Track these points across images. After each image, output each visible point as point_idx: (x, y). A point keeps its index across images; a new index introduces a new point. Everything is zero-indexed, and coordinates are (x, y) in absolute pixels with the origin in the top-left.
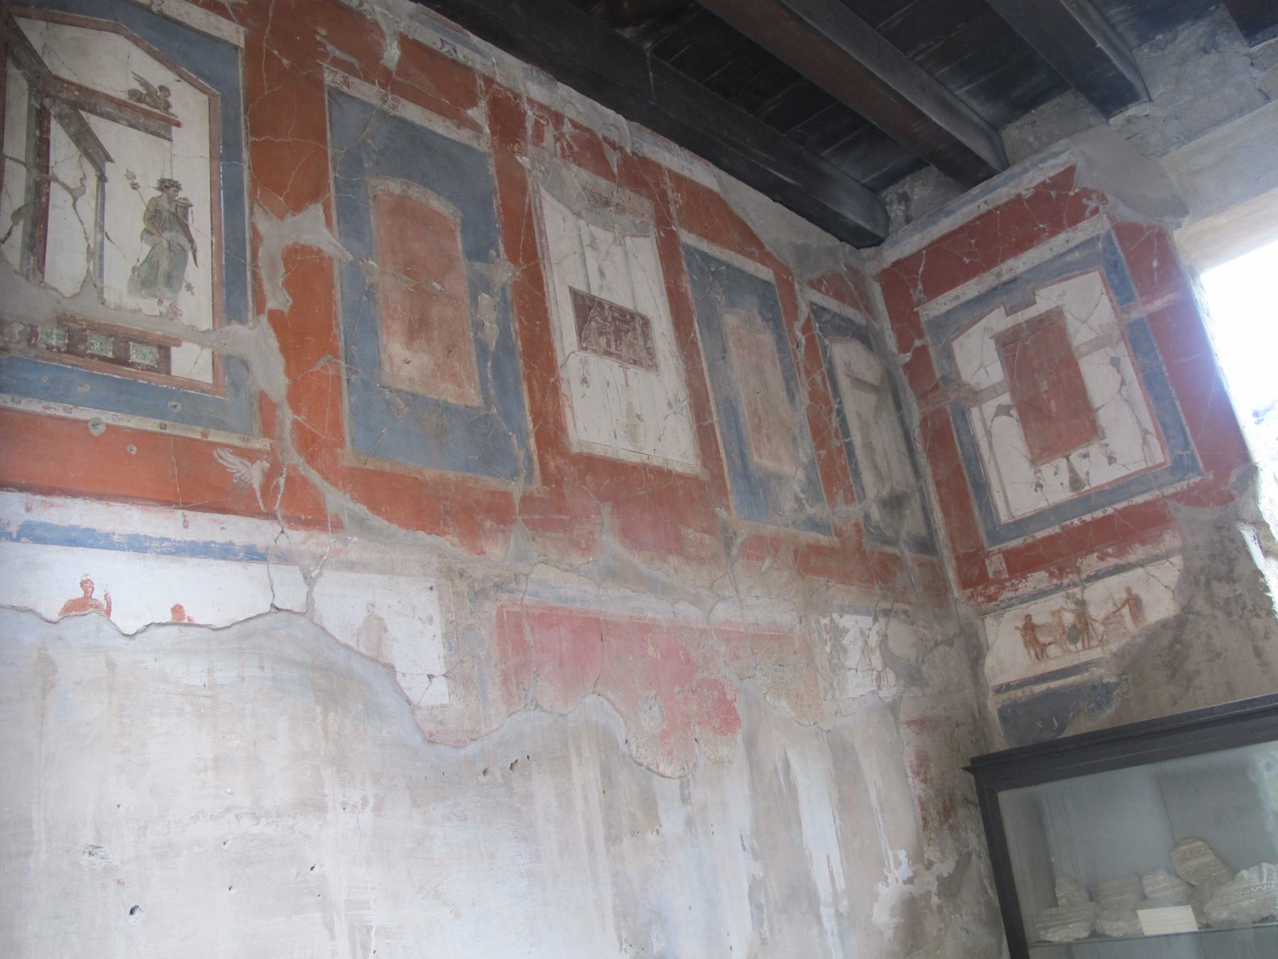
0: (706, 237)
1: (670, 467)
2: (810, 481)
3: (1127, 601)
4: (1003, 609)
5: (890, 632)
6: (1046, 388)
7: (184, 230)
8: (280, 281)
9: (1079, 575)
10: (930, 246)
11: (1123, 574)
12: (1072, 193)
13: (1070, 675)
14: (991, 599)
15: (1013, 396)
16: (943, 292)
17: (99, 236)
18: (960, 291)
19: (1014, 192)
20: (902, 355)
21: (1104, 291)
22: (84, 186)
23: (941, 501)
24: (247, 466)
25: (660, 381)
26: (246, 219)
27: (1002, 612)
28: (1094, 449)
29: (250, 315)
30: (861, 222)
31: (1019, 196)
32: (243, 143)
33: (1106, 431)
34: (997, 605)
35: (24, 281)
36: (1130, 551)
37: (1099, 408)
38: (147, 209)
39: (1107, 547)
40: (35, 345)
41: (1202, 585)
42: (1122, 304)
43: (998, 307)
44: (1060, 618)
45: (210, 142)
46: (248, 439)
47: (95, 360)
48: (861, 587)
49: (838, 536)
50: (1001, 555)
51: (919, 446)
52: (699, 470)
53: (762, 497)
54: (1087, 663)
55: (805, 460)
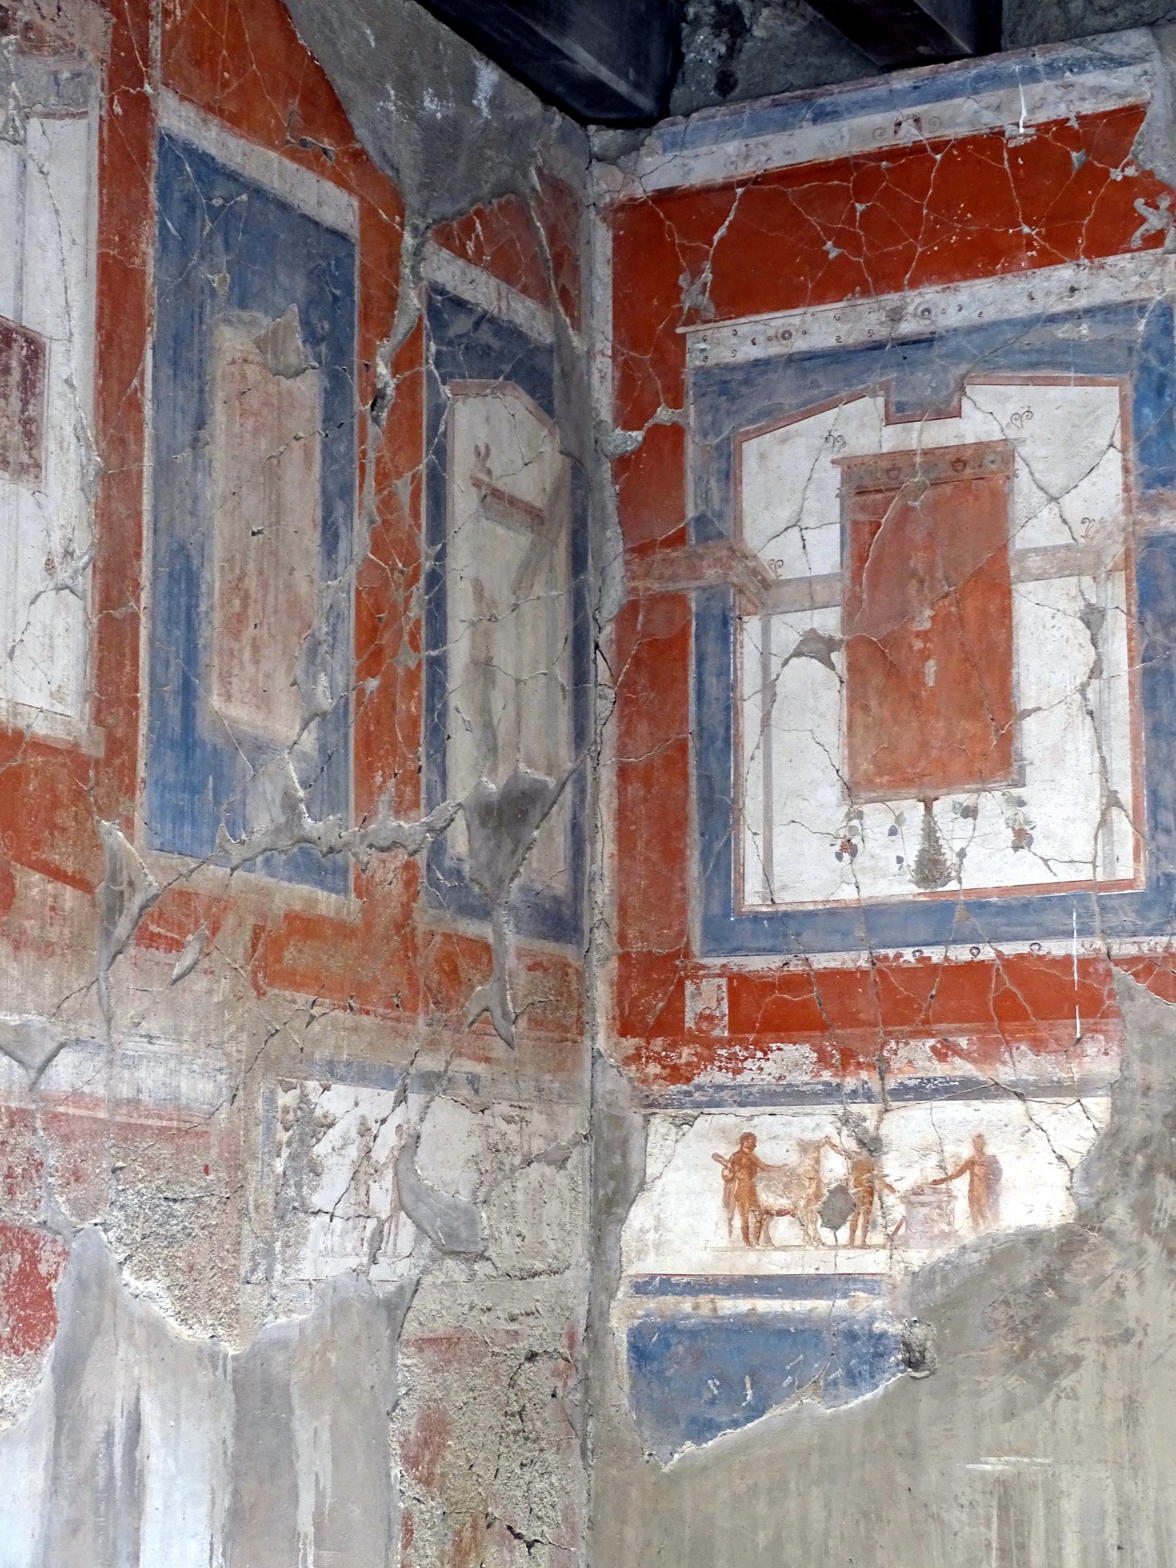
0: (221, 113)
1: (21, 724)
2: (327, 756)
3: (970, 1165)
4: (697, 1105)
5: (426, 1128)
6: (927, 625)
9: (882, 1079)
10: (756, 181)
11: (977, 1103)
12: (1117, 175)
13: (806, 1295)
14: (676, 1074)
15: (848, 619)
16: (758, 312)
18: (796, 321)
19: (990, 119)
20: (618, 431)
21: (1118, 444)
23: (622, 815)
25: (39, 505)
27: (695, 1113)
28: (991, 803)
30: (605, 74)
31: (997, 136)
33: (1028, 769)
34: (688, 1094)
36: (1007, 1055)
37: (1027, 713)
39: (961, 1032)
41: (1135, 1175)
42: (1148, 486)
43: (874, 395)
44: (817, 1161)
48: (384, 1018)
49: (359, 896)
50: (724, 982)
51: (602, 670)
52: (84, 728)
53: (211, 798)
54: (849, 1278)
55: (326, 703)
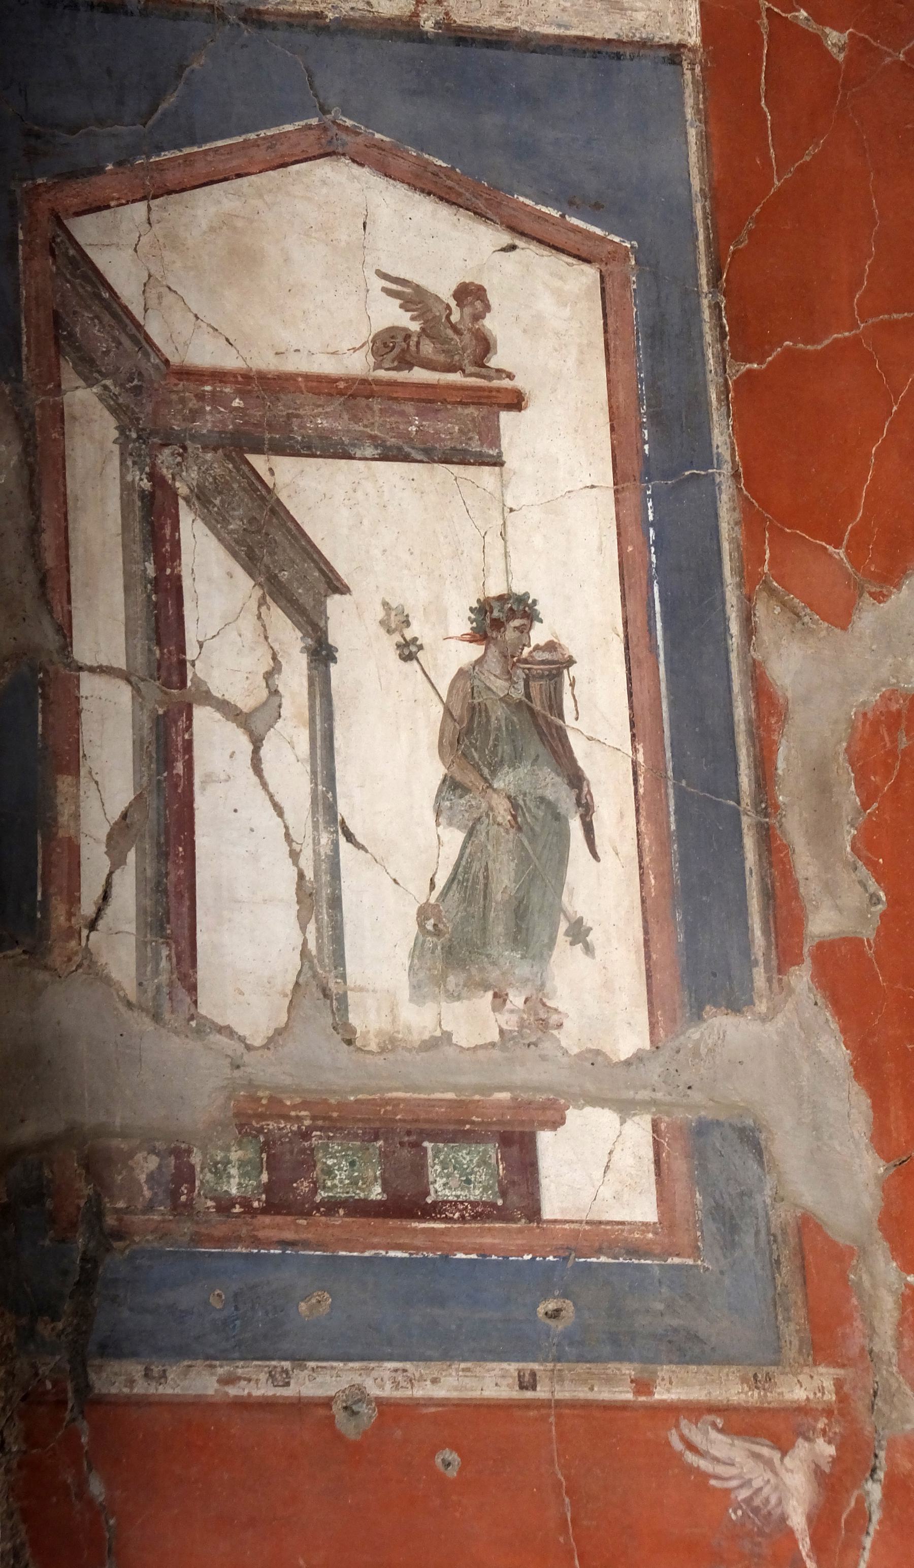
7: (554, 752)
8: (848, 834)
17: (325, 839)
22: (276, 692)
24: (768, 1464)
26: (733, 657)
29: (759, 976)
32: (714, 396)
35: (148, 1025)
38: (448, 711)
40: (189, 1205)
45: (612, 429)
46: (769, 1378)
47: (340, 1219)
